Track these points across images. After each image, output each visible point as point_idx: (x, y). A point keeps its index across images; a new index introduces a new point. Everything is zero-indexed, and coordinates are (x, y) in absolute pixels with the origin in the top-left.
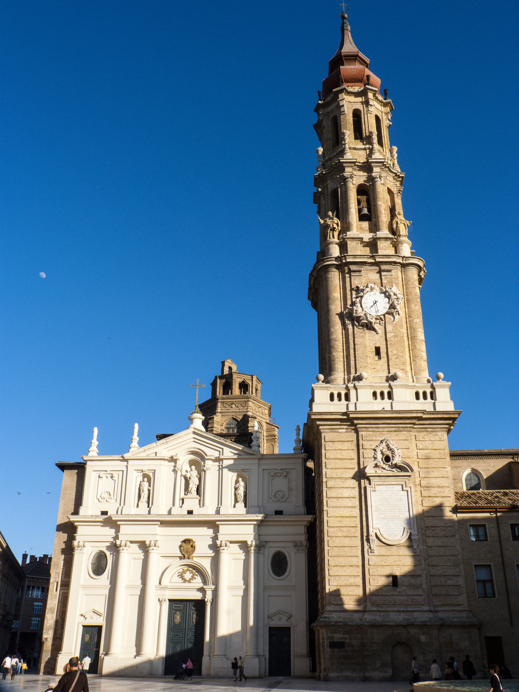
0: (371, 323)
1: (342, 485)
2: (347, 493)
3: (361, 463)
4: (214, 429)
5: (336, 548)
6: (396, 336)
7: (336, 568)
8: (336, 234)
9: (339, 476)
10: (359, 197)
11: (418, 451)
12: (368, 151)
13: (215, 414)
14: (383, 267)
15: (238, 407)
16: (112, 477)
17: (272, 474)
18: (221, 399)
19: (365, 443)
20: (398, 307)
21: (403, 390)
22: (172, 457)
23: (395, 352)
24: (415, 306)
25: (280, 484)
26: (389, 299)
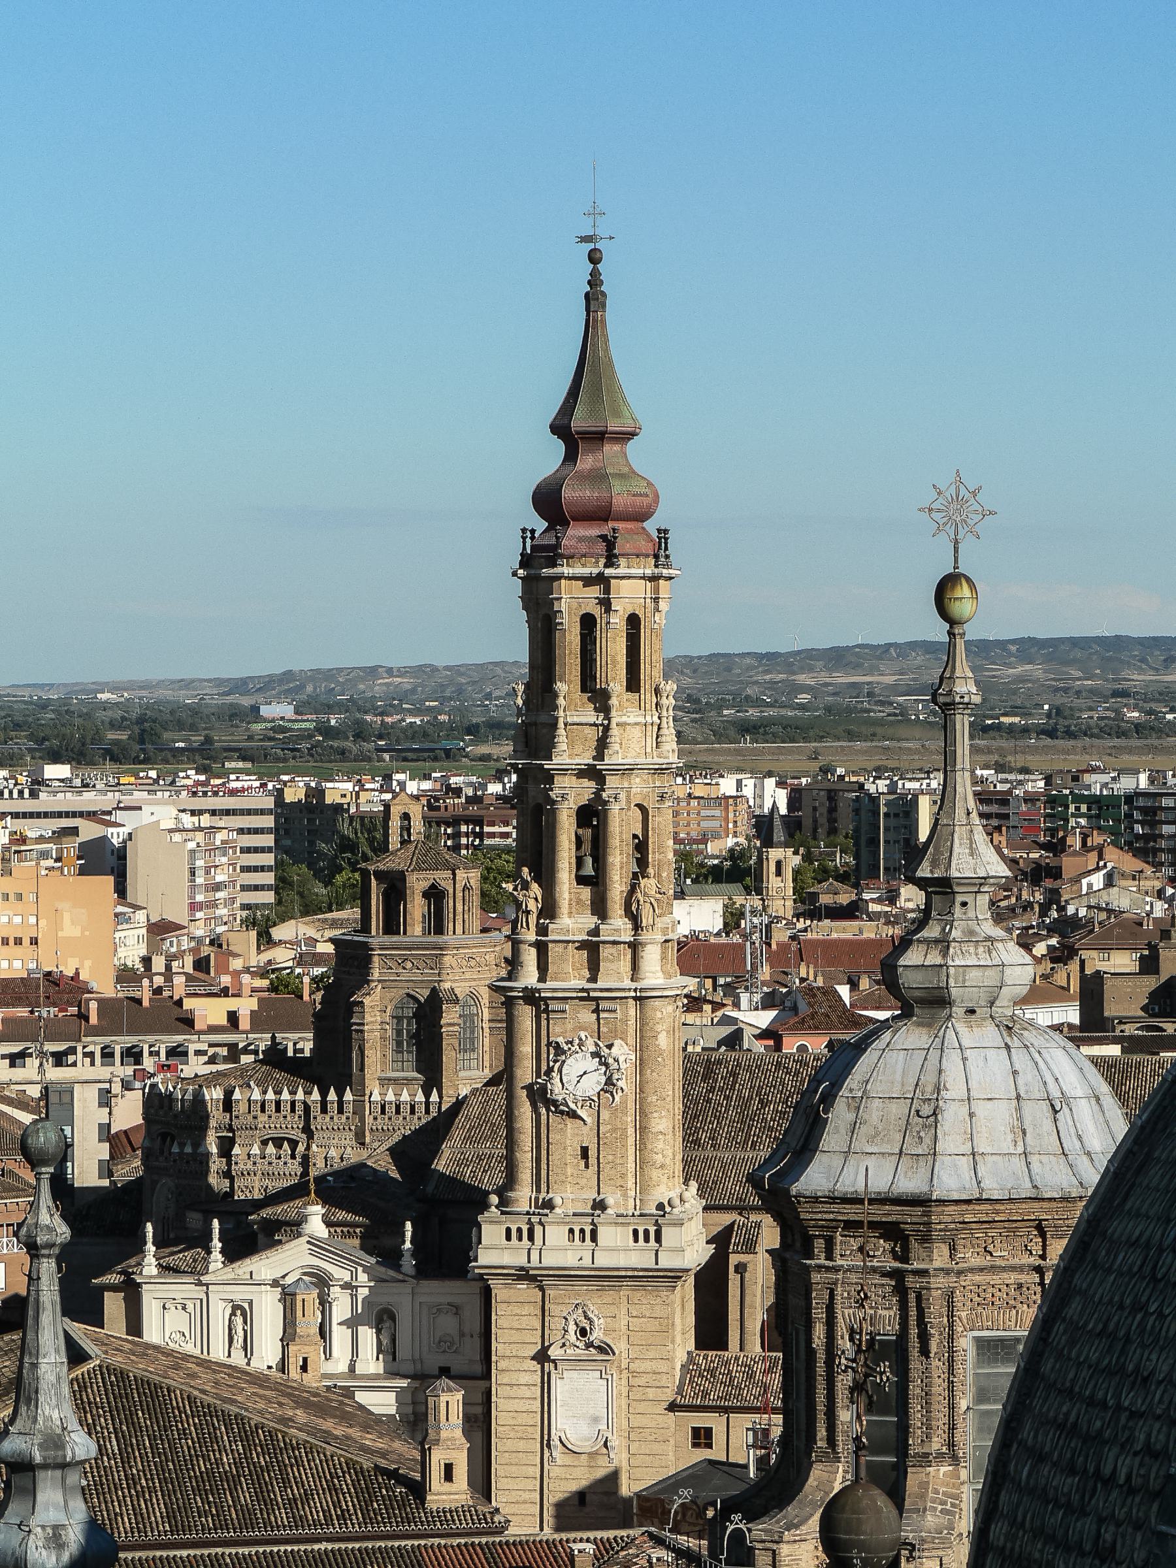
0: (574, 1112)
1: (518, 1366)
2: (525, 1378)
3: (546, 1337)
4: (366, 1028)
5: (507, 1454)
6: (614, 1130)
7: (506, 1480)
8: (533, 919)
9: (514, 1354)
10: (580, 831)
11: (631, 1319)
12: (601, 728)
13: (368, 982)
14: (603, 1005)
15: (418, 969)
16: (184, 1308)
17: (435, 1310)
18: (381, 949)
19: (552, 1307)
20: (620, 1084)
21: (612, 1229)
22: (274, 1280)
23: (610, 1158)
24: (652, 1071)
25: (448, 1324)
26: (607, 1068)
